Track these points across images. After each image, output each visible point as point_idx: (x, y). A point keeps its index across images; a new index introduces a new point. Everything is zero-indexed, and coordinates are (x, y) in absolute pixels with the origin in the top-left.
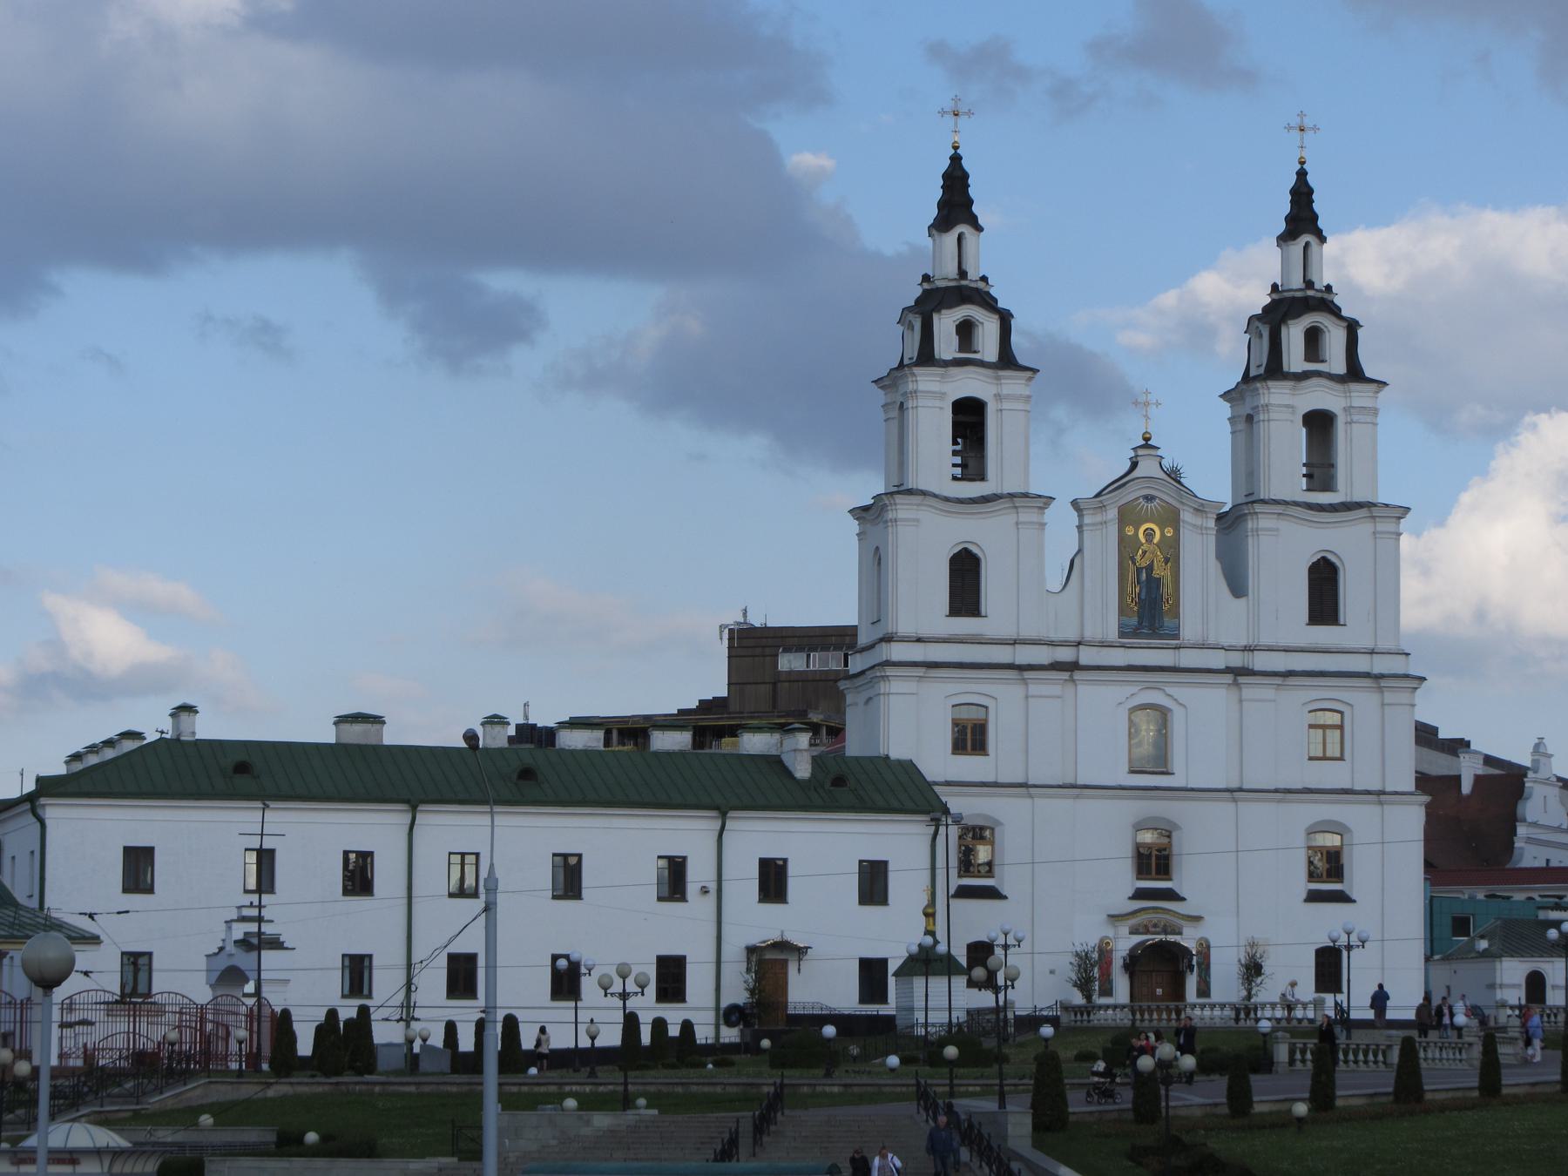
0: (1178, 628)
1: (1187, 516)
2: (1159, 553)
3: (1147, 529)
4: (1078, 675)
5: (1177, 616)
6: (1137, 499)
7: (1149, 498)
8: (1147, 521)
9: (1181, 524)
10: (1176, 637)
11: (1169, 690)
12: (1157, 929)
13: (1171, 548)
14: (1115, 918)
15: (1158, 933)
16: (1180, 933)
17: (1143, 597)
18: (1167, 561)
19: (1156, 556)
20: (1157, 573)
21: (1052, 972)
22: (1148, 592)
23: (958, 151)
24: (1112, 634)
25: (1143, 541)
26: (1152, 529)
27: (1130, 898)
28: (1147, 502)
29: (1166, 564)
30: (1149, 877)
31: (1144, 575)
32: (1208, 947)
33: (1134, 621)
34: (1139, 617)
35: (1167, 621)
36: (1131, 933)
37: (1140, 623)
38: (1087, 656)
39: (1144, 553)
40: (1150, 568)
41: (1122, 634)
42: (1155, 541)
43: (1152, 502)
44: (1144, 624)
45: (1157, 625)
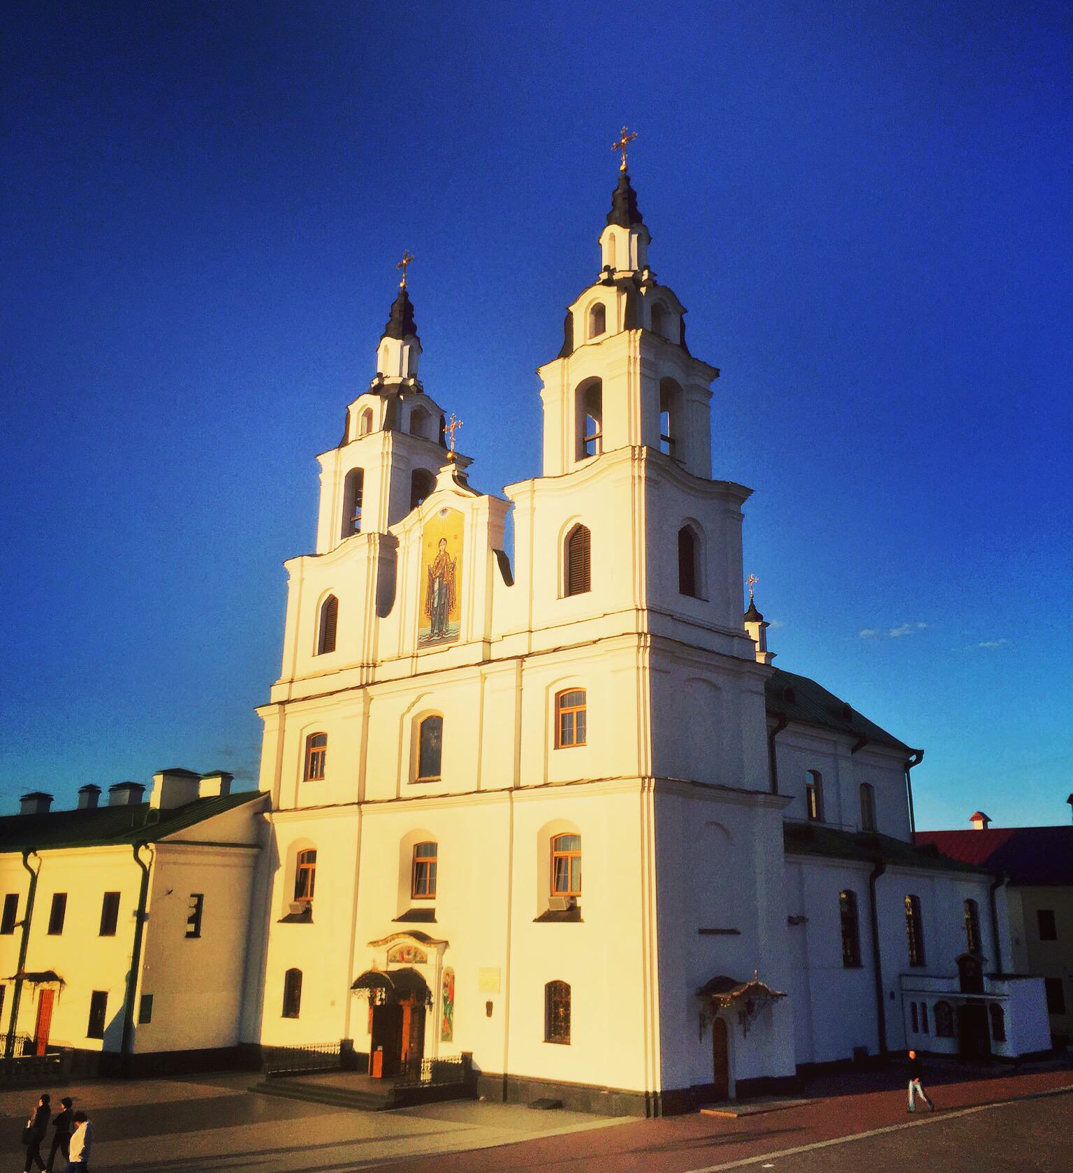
0: (458, 630)
1: (468, 519)
5: (459, 618)
7: (444, 511)
10: (456, 638)
12: (411, 957)
13: (457, 552)
14: (374, 943)
15: (411, 962)
16: (425, 962)
17: (435, 606)
20: (448, 577)
21: (333, 1004)
24: (410, 646)
27: (394, 920)
30: (424, 896)
32: (453, 978)
33: (428, 630)
34: (433, 626)
35: (452, 624)
36: (392, 961)
37: (432, 631)
40: (442, 575)
41: (421, 645)
44: (435, 631)
45: (444, 630)
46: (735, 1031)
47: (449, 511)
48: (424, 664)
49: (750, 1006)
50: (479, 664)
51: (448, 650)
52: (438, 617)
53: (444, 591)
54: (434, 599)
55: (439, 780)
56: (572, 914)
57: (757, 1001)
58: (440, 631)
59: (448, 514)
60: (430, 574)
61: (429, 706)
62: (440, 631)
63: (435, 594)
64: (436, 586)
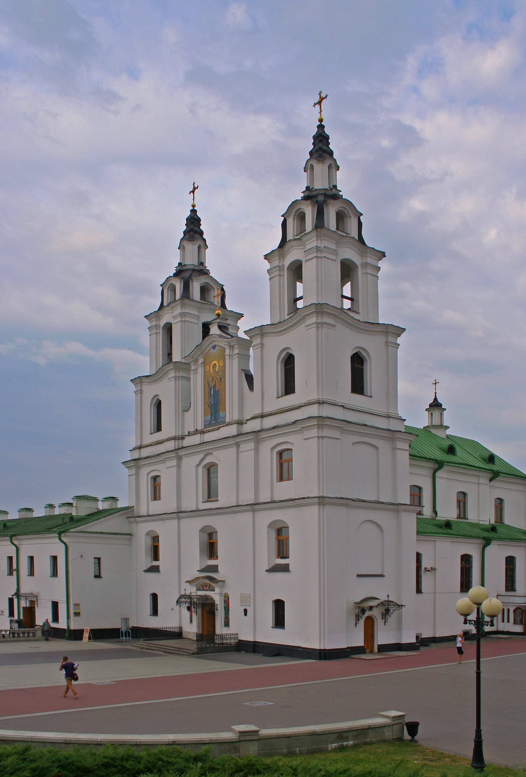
1: (227, 352)
2: (218, 377)
3: (213, 365)
4: (181, 453)
5: (225, 410)
6: (210, 349)
8: (213, 361)
9: (226, 357)
11: (215, 453)
17: (212, 403)
18: (221, 379)
19: (217, 378)
20: (218, 387)
22: (214, 400)
23: (195, 208)
25: (212, 372)
26: (215, 364)
28: (213, 350)
29: (220, 382)
31: (212, 390)
33: (209, 418)
34: (211, 415)
35: (221, 414)
37: (211, 418)
38: (188, 441)
39: (213, 378)
40: (215, 386)
41: (206, 426)
42: (217, 370)
43: (215, 349)
44: (213, 418)
45: (217, 417)
46: (379, 623)
47: (217, 347)
48: (209, 437)
49: (387, 611)
50: (234, 437)
51: (219, 429)
52: (214, 410)
53: (216, 395)
54: (211, 399)
55: (217, 500)
56: (285, 568)
57: (392, 608)
58: (215, 417)
59: (216, 349)
60: (208, 383)
61: (209, 460)
62: (215, 417)
63: (212, 397)
64: (212, 393)
